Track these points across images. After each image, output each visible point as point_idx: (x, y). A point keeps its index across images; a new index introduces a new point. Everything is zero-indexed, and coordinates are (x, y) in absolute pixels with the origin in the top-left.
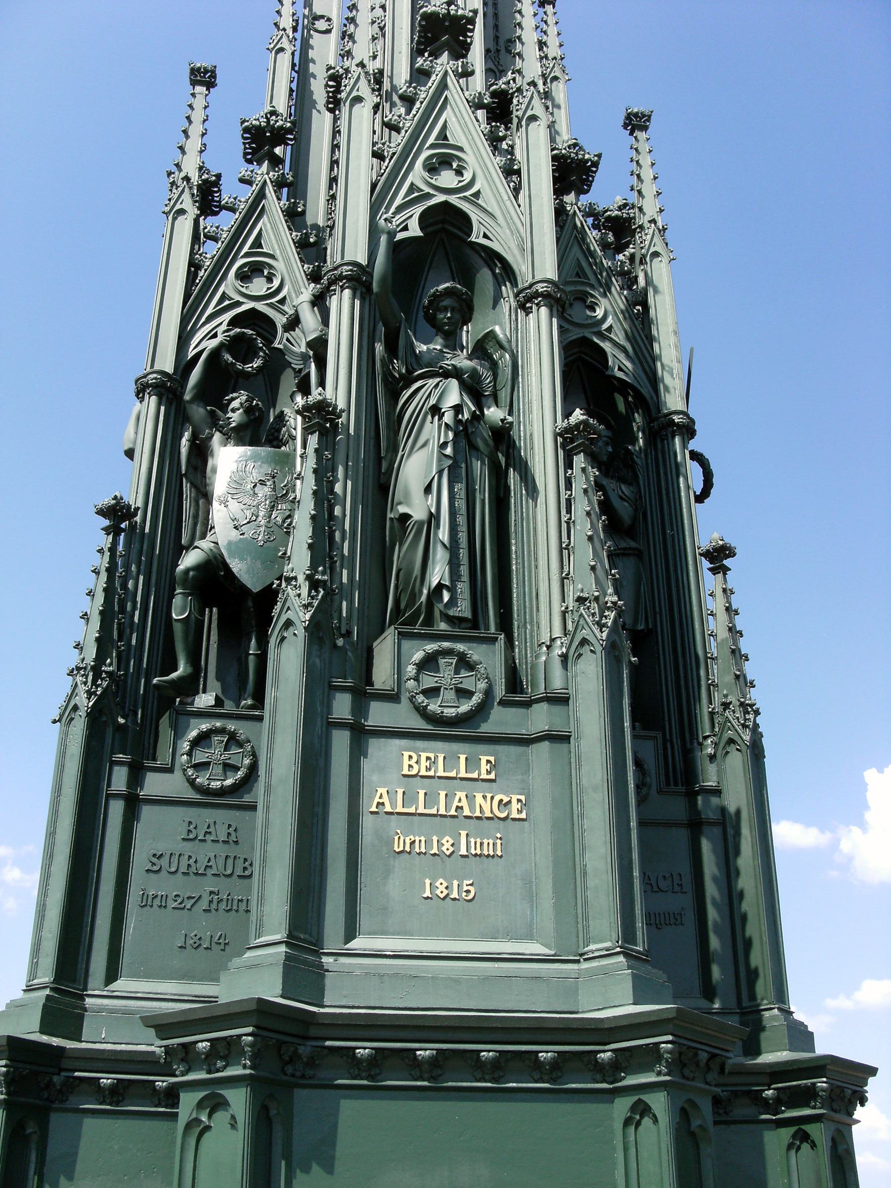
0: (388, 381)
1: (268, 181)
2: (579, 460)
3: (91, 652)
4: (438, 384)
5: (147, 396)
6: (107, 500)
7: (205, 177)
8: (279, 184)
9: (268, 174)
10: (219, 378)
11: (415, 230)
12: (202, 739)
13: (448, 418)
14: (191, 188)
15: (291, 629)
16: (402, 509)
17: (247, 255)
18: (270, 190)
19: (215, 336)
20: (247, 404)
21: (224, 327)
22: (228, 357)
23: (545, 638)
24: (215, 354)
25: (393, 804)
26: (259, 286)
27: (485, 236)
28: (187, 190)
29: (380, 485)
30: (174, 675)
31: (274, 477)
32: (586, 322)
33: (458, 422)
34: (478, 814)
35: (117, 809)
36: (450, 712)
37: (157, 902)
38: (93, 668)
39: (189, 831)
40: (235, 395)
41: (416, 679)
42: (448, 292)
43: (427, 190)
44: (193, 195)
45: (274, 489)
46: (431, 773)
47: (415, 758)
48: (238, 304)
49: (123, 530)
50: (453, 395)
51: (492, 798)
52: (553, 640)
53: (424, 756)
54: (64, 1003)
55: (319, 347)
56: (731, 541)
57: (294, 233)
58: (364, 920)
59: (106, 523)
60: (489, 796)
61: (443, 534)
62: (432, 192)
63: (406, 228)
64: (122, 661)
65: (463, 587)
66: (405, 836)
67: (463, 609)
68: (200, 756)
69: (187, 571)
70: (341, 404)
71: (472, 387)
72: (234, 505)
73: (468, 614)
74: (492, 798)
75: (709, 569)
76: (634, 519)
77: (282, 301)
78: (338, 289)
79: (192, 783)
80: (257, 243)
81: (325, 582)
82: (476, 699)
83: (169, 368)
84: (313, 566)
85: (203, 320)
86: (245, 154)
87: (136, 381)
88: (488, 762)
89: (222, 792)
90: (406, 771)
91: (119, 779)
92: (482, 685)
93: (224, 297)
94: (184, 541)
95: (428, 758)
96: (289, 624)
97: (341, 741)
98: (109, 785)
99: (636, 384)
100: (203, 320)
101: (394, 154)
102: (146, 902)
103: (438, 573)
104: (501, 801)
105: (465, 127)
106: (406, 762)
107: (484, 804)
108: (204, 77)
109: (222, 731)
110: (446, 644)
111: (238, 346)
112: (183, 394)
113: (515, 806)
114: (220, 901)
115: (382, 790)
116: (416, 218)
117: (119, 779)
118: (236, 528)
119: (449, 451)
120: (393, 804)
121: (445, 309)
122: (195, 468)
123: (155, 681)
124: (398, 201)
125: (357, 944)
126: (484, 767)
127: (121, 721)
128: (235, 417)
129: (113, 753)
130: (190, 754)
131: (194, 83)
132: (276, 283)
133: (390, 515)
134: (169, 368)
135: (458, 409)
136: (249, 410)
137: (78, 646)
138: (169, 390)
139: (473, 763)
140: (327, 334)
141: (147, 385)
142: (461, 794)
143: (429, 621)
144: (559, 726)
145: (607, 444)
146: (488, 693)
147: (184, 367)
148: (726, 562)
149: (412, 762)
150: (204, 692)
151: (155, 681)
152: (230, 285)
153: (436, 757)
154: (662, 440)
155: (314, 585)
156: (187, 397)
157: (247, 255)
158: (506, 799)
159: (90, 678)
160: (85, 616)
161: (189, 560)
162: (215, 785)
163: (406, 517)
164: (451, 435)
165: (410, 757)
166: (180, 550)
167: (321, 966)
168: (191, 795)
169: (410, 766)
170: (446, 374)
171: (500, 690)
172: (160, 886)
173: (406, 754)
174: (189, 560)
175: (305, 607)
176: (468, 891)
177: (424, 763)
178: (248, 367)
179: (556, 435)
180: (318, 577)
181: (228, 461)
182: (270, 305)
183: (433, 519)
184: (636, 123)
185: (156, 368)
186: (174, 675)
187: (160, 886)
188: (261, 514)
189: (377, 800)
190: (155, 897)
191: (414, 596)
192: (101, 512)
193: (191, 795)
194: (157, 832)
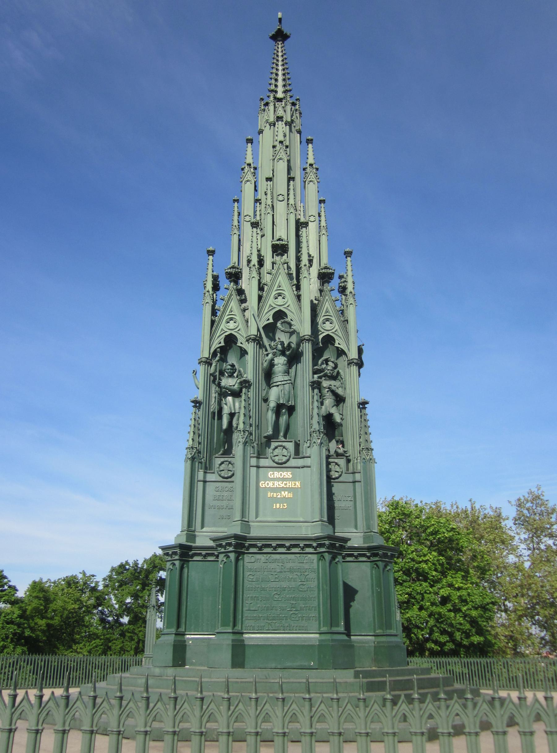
6: (193, 399)
18: (234, 293)
35: (201, 484)
41: (272, 453)
43: (274, 306)
54: (191, 534)
56: (367, 399)
58: (261, 513)
59: (193, 404)
62: (276, 306)
63: (268, 320)
68: (221, 468)
82: (287, 458)
91: (200, 475)
92: (289, 454)
93: (222, 330)
107: (290, 484)
109: (227, 461)
125: (258, 519)
131: (209, 255)
132: (236, 324)
134: (207, 356)
141: (202, 362)
148: (366, 406)
152: (223, 326)
162: (226, 476)
167: (249, 525)
171: (293, 456)
179: (309, 382)
192: (193, 402)
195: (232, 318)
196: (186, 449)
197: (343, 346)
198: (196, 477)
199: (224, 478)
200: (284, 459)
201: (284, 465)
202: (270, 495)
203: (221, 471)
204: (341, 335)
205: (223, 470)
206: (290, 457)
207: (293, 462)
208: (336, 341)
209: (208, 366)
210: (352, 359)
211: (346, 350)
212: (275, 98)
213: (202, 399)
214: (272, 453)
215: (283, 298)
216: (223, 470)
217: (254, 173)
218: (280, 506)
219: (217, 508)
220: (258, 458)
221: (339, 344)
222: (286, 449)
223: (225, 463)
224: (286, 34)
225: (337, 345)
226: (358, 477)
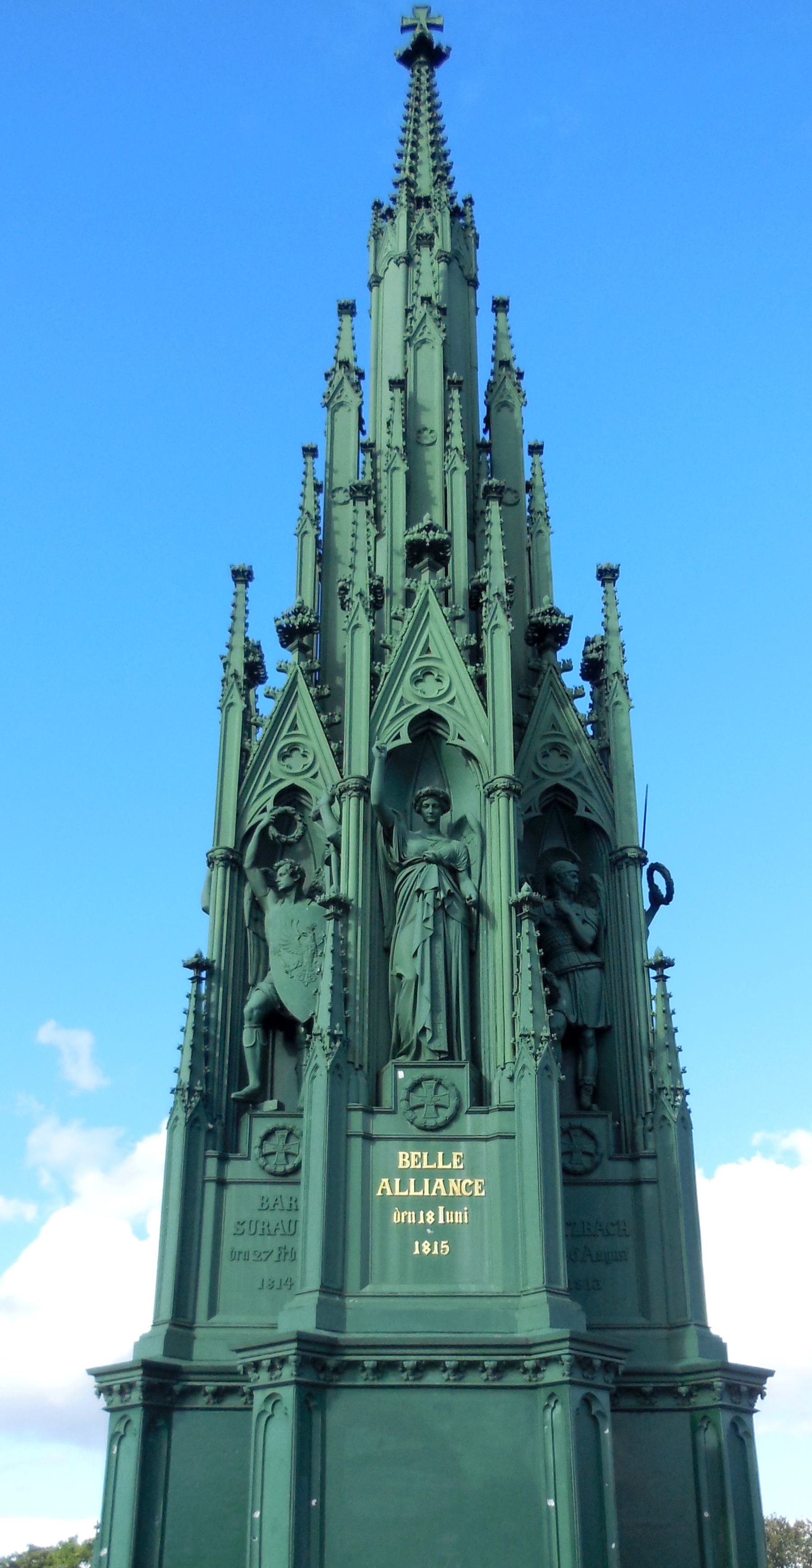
0: (385, 872)
1: (299, 671)
2: (526, 924)
3: (186, 1076)
4: (422, 870)
5: (215, 867)
7: (251, 658)
8: (309, 672)
9: (299, 664)
10: (270, 851)
11: (405, 739)
12: (268, 1135)
13: (429, 899)
14: (238, 684)
15: (318, 1070)
16: (398, 970)
17: (286, 737)
19: (265, 810)
20: (291, 871)
21: (270, 805)
22: (273, 832)
23: (500, 1063)
24: (265, 830)
25: (392, 1190)
26: (296, 762)
27: (460, 737)
28: (235, 685)
29: (383, 950)
30: (246, 1090)
31: (313, 929)
32: (559, 770)
33: (436, 900)
34: (451, 1194)
35: (210, 1190)
36: (431, 1123)
37: (242, 1256)
38: (188, 1089)
39: (262, 1204)
40: (282, 862)
41: (408, 1100)
42: (429, 795)
44: (240, 689)
45: (314, 940)
46: (419, 1166)
47: (407, 1156)
48: (281, 780)
49: (203, 979)
50: (432, 877)
51: (461, 1182)
52: (505, 1064)
53: (413, 1154)
55: (335, 841)
57: (322, 716)
59: (191, 973)
60: (459, 1180)
61: (425, 990)
62: (418, 703)
64: (207, 1078)
65: (442, 1028)
66: (401, 1211)
67: (441, 1044)
68: (268, 1148)
69: (252, 1011)
70: (351, 896)
71: (450, 867)
72: (286, 955)
73: (444, 1047)
74: (461, 1182)
75: (654, 978)
76: (596, 940)
77: (314, 776)
78: (347, 798)
79: (263, 1168)
80: (294, 726)
81: (341, 1035)
83: (230, 844)
84: (332, 1026)
85: (254, 797)
86: (281, 643)
87: (207, 854)
88: (458, 1156)
89: (285, 1174)
90: (401, 1166)
91: (211, 1168)
92: (453, 1102)
94: (250, 980)
95: (416, 1156)
96: (316, 1067)
97: (356, 1145)
98: (204, 1173)
99: (600, 823)
100: (254, 797)
101: (387, 674)
102: (235, 1255)
103: (423, 1017)
104: (467, 1184)
105: (443, 639)
106: (401, 1160)
107: (456, 1187)
108: (242, 576)
110: (427, 1072)
111: (283, 822)
112: (242, 862)
113: (477, 1187)
114: (286, 1254)
115: (385, 1180)
116: (406, 725)
117: (212, 1166)
118: (287, 972)
119: (430, 924)
120: (392, 1190)
121: (428, 806)
122: (256, 920)
123: (233, 1095)
124: (391, 715)
126: (455, 1161)
127: (211, 1126)
128: (283, 881)
129: (206, 1150)
130: (261, 1147)
133: (390, 973)
135: (436, 890)
136: (293, 875)
137: (177, 1071)
138: (233, 861)
139: (447, 1159)
140: (340, 831)
142: (440, 1181)
143: (417, 1056)
144: (507, 1128)
145: (574, 877)
146: (458, 1108)
147: (243, 840)
148: (666, 972)
149: (406, 1160)
150: (272, 1099)
151: (233, 1095)
153: (422, 1155)
154: (619, 870)
155: (334, 1038)
156: (247, 864)
157: (286, 737)
158: (470, 1183)
159: (186, 1098)
160: (180, 1047)
161: (255, 999)
162: (280, 1169)
163: (400, 976)
164: (431, 911)
165: (404, 1156)
166: (246, 989)
168: (264, 1177)
169: (404, 1163)
170: (429, 861)
172: (246, 1243)
173: (401, 1154)
174: (255, 999)
175: (327, 1055)
176: (444, 1249)
177: (414, 1160)
178: (291, 838)
179: (510, 906)
180: (336, 1032)
181: (280, 916)
182: (305, 780)
183: (418, 980)
184: (607, 575)
185: (222, 844)
186: (246, 1090)
187: (246, 1243)
188: (305, 960)
189: (381, 1187)
190: (240, 1253)
191: (408, 1035)
193: (264, 1177)
194: (240, 1204)
195: (295, 744)
196: (172, 1092)
197: (598, 816)
198: (200, 1173)
199: (274, 1174)
200: (445, 1114)
201: (445, 1133)
202: (397, 1217)
203: (265, 1156)
204: (591, 787)
205: (273, 1154)
206: (458, 1108)
207: (468, 1124)
208: (580, 801)
209: (233, 870)
210: (622, 849)
211: (606, 827)
212: (410, 198)
213: (215, 957)
214: (408, 1100)
215: (438, 680)
216: (273, 1154)
217: (358, 384)
218: (431, 1247)
219: (252, 1257)
220: (368, 1112)
221: (587, 810)
222: (447, 1088)
223: (278, 1134)
224: (439, 48)
225: (581, 812)
226: (647, 1168)
